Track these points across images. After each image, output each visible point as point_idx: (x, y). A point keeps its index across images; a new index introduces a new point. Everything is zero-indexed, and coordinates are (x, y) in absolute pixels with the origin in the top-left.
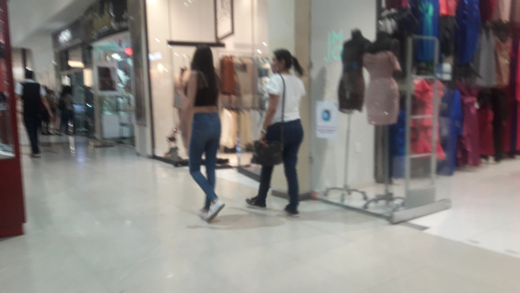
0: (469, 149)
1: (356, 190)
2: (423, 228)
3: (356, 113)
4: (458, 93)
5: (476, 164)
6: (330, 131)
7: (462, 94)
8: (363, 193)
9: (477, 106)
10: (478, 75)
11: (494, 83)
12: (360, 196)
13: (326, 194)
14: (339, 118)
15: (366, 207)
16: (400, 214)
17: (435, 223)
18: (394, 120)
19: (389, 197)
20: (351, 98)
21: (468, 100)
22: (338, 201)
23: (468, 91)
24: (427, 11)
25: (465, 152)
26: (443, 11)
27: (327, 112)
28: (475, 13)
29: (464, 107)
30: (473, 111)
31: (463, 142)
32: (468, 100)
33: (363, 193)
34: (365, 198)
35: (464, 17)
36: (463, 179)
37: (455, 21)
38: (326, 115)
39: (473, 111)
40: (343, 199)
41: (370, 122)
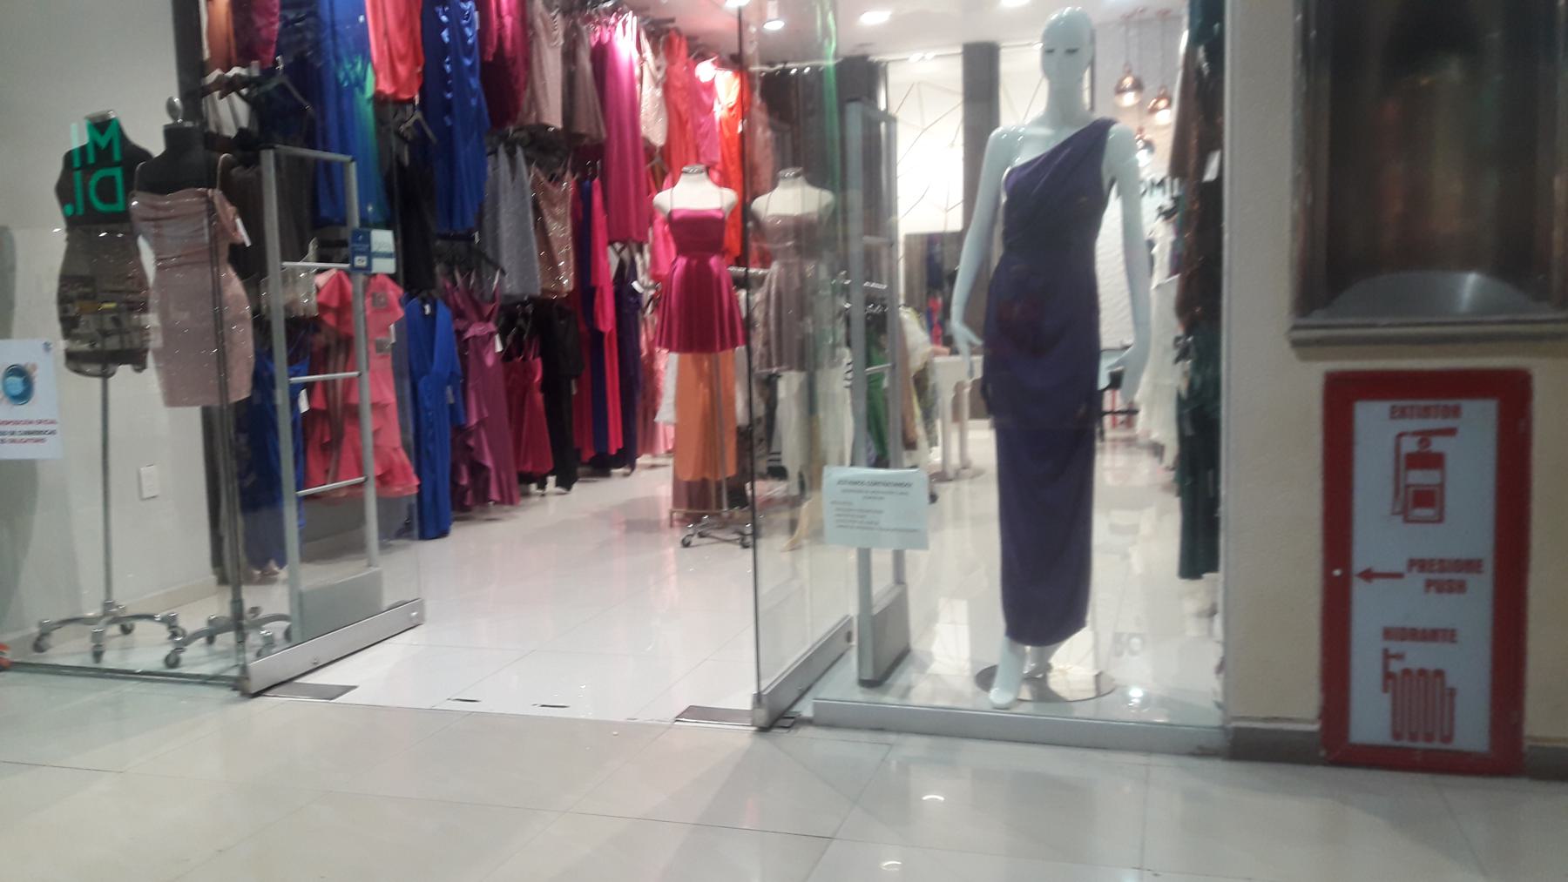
0: (489, 463)
1: (151, 617)
2: (331, 693)
3: (124, 371)
4: (444, 314)
5: (508, 500)
6: (36, 436)
7: (459, 314)
8: (170, 622)
9: (499, 348)
10: (496, 266)
11: (539, 293)
12: (163, 631)
13: (39, 646)
14: (63, 392)
15: (172, 661)
16: (262, 668)
17: (375, 674)
18: (241, 389)
19: (238, 623)
20: (101, 328)
21: (476, 330)
22: (87, 660)
23: (474, 306)
24: (360, 83)
25: (477, 469)
26: (387, 88)
27: (17, 371)
28: (474, 102)
29: (467, 349)
30: (490, 361)
31: (471, 442)
32: (476, 330)
33: (170, 622)
34: (174, 635)
35: (448, 107)
36: (465, 538)
37: (418, 115)
38: (16, 384)
39: (490, 361)
40: (98, 655)
41: (173, 398)
